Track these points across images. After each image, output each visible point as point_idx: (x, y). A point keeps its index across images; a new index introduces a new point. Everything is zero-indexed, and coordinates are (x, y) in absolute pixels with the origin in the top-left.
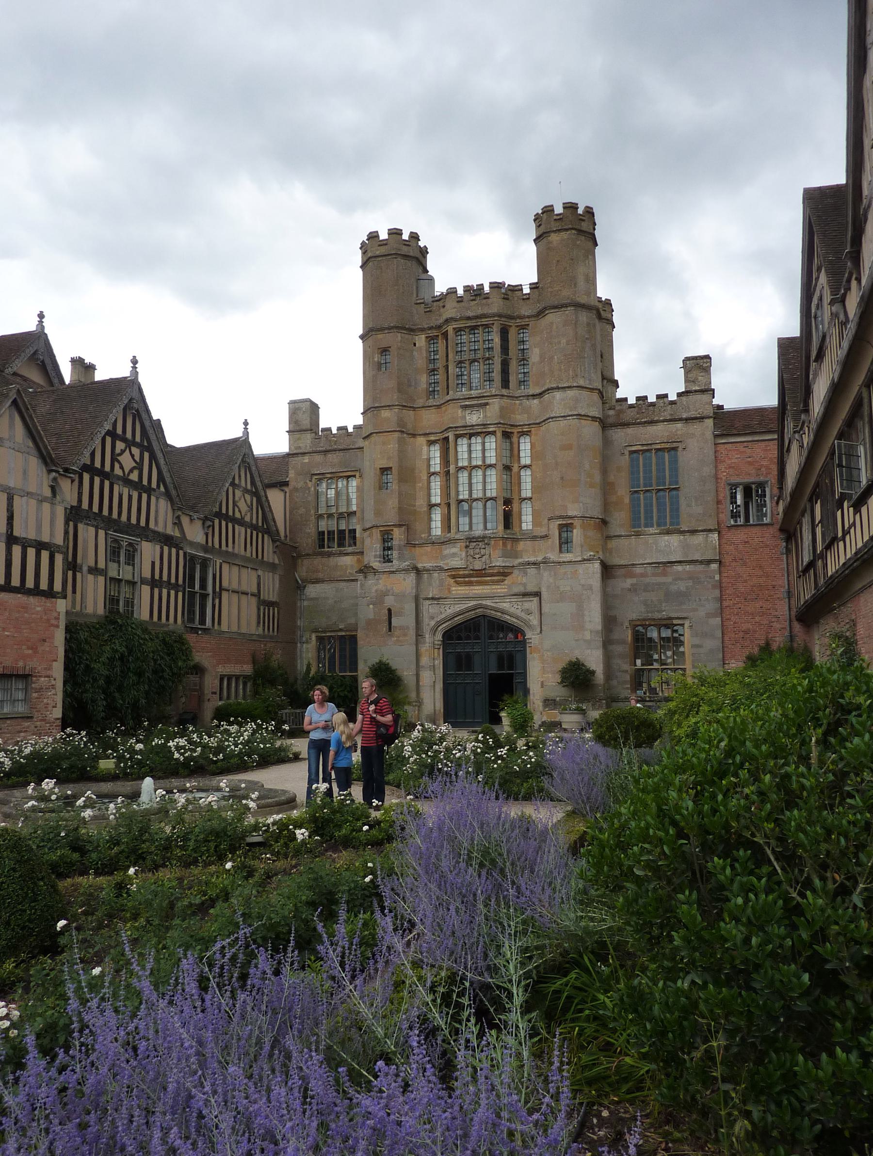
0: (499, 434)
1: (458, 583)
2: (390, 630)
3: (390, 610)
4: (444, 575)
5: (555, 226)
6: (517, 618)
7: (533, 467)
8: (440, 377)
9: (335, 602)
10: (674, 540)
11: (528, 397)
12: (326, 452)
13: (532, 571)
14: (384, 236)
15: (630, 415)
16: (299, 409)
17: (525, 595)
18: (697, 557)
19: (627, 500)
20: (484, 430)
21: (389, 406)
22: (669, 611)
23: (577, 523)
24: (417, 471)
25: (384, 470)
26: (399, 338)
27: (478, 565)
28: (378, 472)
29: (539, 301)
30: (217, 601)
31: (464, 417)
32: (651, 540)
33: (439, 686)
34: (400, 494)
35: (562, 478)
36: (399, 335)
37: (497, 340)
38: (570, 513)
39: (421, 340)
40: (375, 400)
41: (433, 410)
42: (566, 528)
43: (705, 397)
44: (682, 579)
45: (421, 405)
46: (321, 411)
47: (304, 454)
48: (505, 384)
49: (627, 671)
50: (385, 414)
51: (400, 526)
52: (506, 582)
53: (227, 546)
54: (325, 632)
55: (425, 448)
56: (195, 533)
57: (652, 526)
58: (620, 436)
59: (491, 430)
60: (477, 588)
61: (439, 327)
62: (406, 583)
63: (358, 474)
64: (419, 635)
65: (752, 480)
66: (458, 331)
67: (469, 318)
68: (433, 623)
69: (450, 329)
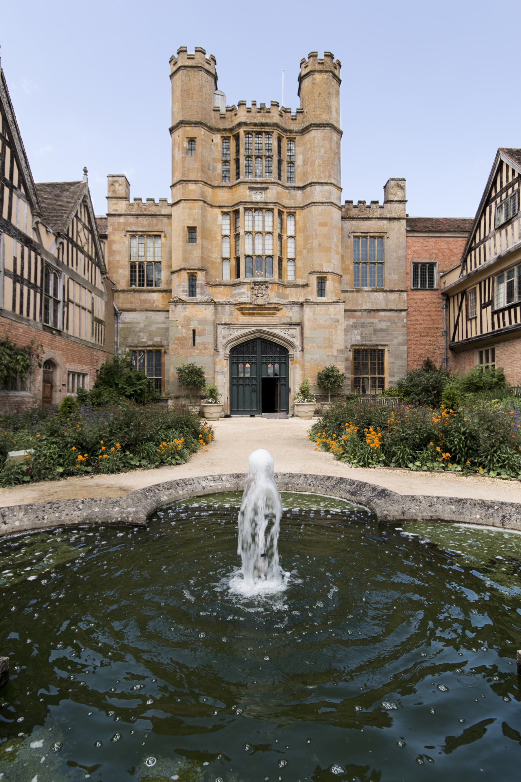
0: (276, 211)
1: (243, 314)
2: (194, 344)
3: (194, 331)
4: (233, 308)
5: (318, 67)
6: (285, 340)
7: (297, 238)
8: (232, 166)
9: (145, 325)
10: (380, 296)
11: (294, 188)
12: (137, 215)
13: (296, 309)
15: (354, 212)
16: (117, 181)
17: (291, 324)
18: (394, 307)
19: (351, 267)
20: (266, 207)
21: (195, 181)
22: (376, 340)
23: (329, 276)
24: (213, 233)
25: (192, 230)
26: (203, 133)
27: (260, 302)
28: (186, 229)
29: (303, 122)
30: (66, 309)
31: (250, 196)
32: (366, 295)
33: (227, 386)
34: (203, 247)
35: (320, 245)
36: (203, 130)
37: (276, 144)
38: (325, 270)
39: (217, 138)
40: (183, 175)
41: (226, 190)
42: (322, 281)
43: (401, 205)
44: (385, 321)
45: (216, 185)
46: (131, 187)
47: (120, 215)
48: (280, 177)
49: (349, 378)
50: (192, 186)
51: (202, 270)
52: (278, 315)
53: (72, 266)
54: (137, 347)
55: (220, 217)
56: (49, 243)
57: (366, 286)
58: (350, 225)
59: (270, 207)
60: (257, 318)
61: (231, 130)
62: (208, 312)
63: (163, 235)
64: (216, 350)
65: (427, 261)
66: (247, 133)
67: (255, 125)
68: (225, 341)
69: (241, 131)
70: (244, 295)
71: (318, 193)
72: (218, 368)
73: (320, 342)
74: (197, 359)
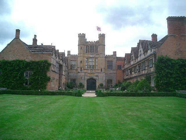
10: (112, 71)
14: (82, 34)
22: (111, 78)
25: (81, 61)
58: (106, 59)
62: (83, 74)
70: (89, 72)
71: (101, 56)
72: (85, 83)
73: (101, 79)
74: (82, 82)
